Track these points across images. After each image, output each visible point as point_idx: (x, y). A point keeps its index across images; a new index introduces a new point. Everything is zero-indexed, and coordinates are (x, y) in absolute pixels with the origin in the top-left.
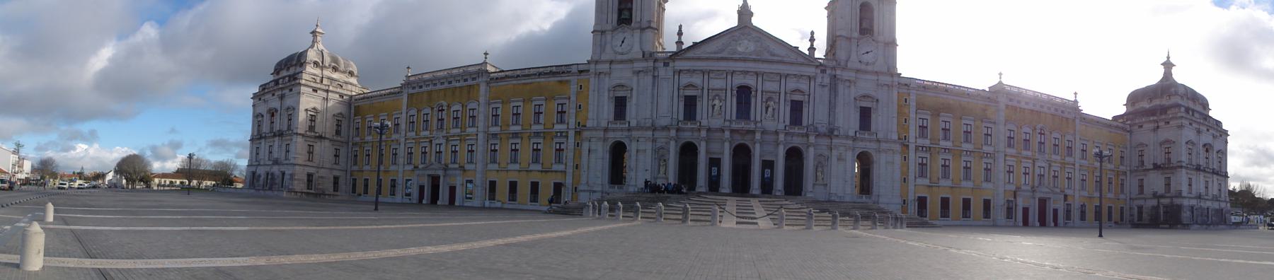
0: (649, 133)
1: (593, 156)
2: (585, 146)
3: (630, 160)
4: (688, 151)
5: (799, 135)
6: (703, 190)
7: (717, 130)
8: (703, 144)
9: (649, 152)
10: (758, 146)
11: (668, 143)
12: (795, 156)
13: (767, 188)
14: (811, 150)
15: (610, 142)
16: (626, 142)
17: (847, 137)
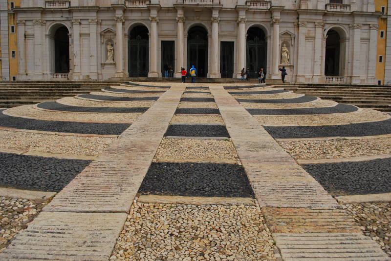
0: (93, 15)
1: (30, 42)
2: (21, 30)
3: (75, 48)
4: (139, 34)
5: (260, 12)
6: (156, 76)
7: (168, 10)
8: (154, 25)
9: (93, 36)
10: (216, 26)
11: (114, 26)
12: (257, 36)
13: (227, 71)
14: (277, 27)
15: (49, 26)
16: (67, 25)
17: (316, 12)
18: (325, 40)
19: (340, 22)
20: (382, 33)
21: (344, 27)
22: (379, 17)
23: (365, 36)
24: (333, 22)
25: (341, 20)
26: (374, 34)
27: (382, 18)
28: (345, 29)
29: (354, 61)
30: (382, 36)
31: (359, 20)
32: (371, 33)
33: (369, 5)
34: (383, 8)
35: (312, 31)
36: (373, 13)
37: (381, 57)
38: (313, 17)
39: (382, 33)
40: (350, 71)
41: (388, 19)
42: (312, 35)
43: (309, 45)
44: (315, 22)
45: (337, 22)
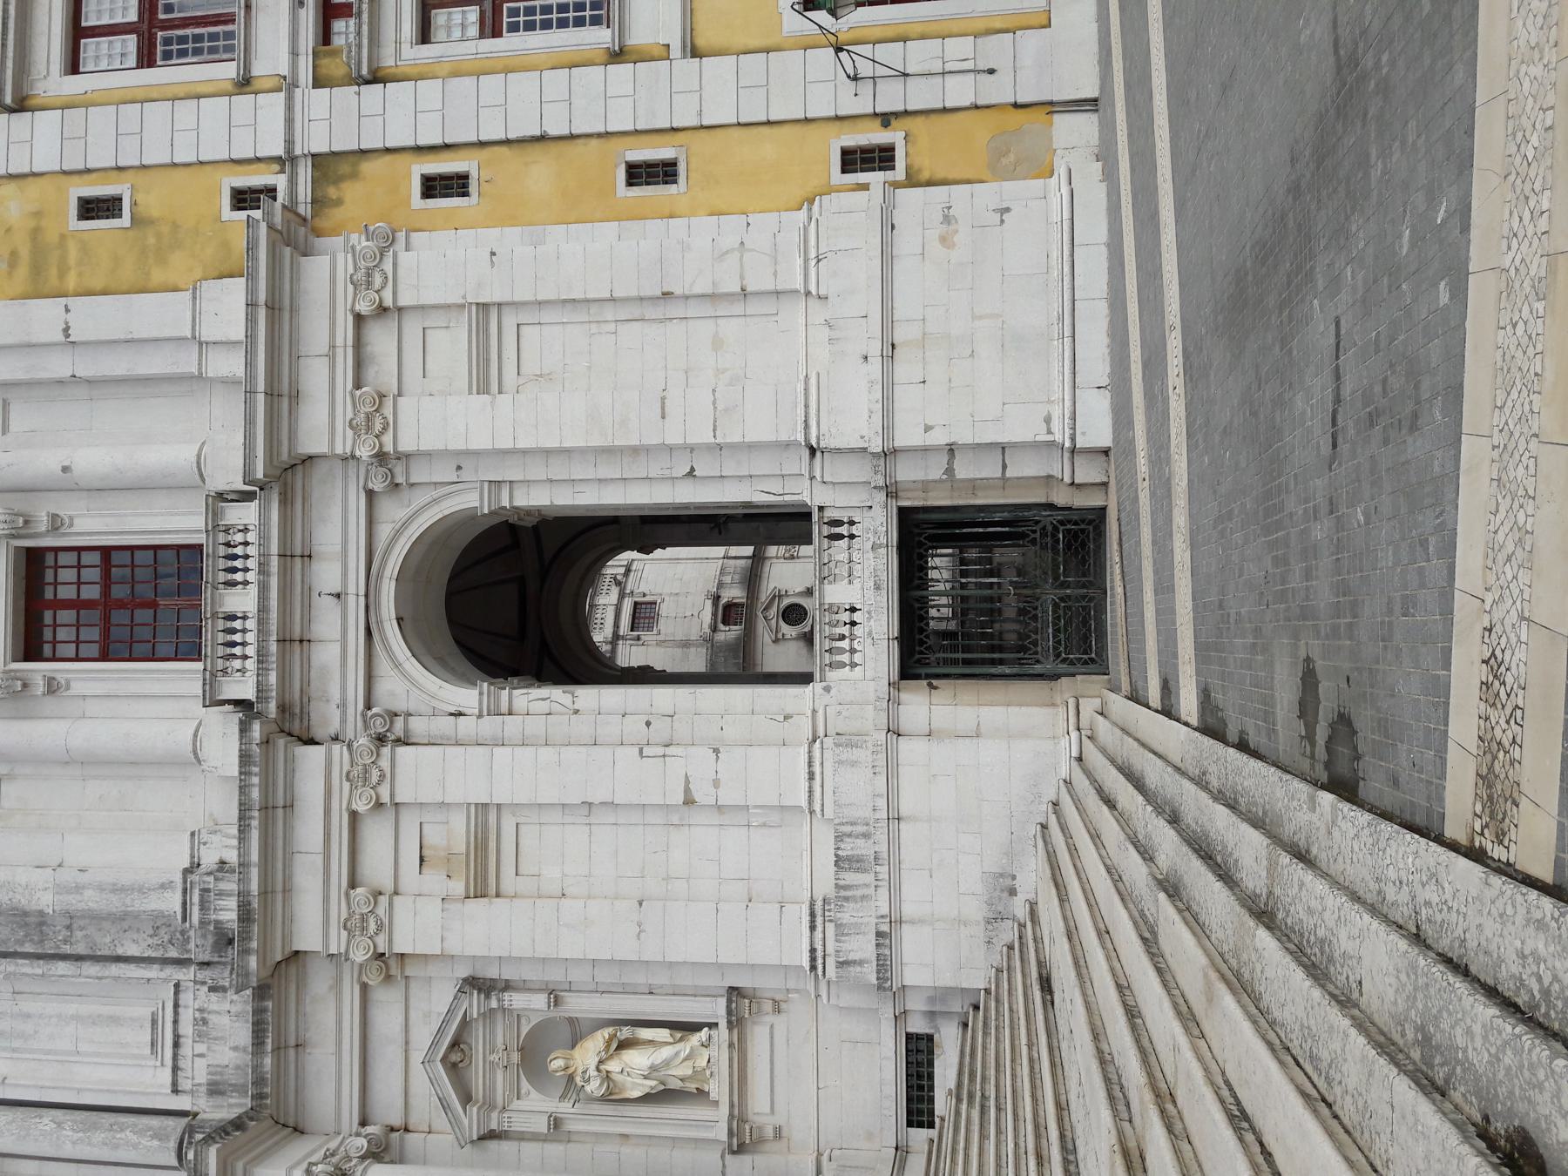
17: (266, 809)
18: (505, 693)
19: (356, 584)
20: (433, 187)
21: (398, 534)
22: (296, 236)
23: (451, 347)
24: (356, 637)
25: (336, 563)
26: (443, 260)
27: (318, 202)
28: (412, 519)
29: (674, 439)
30: (455, 185)
31: (322, 425)
32: (429, 298)
33: (207, 334)
34: (243, 199)
35: (434, 837)
36: (251, 305)
37: (639, 174)
38: (309, 830)
39: (433, 187)
40: (762, 464)
41: (320, 146)
42: (453, 834)
43: (549, 854)
44: (354, 816)
45: (355, 605)
